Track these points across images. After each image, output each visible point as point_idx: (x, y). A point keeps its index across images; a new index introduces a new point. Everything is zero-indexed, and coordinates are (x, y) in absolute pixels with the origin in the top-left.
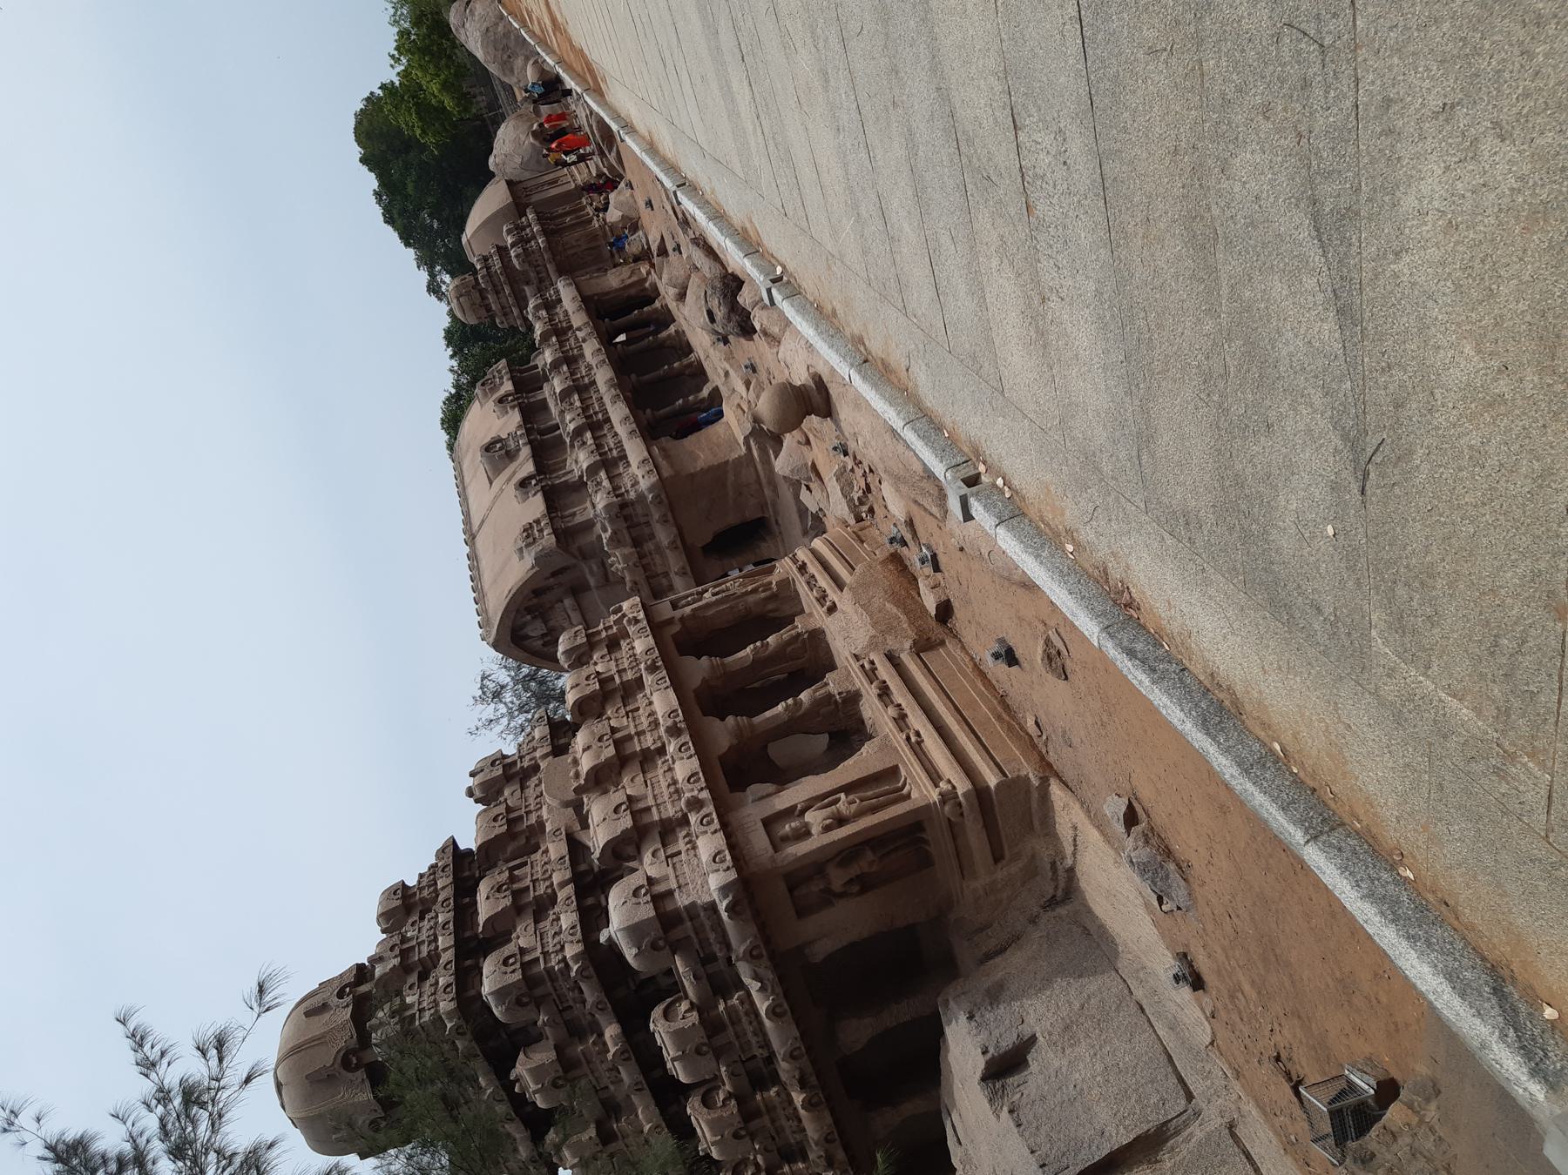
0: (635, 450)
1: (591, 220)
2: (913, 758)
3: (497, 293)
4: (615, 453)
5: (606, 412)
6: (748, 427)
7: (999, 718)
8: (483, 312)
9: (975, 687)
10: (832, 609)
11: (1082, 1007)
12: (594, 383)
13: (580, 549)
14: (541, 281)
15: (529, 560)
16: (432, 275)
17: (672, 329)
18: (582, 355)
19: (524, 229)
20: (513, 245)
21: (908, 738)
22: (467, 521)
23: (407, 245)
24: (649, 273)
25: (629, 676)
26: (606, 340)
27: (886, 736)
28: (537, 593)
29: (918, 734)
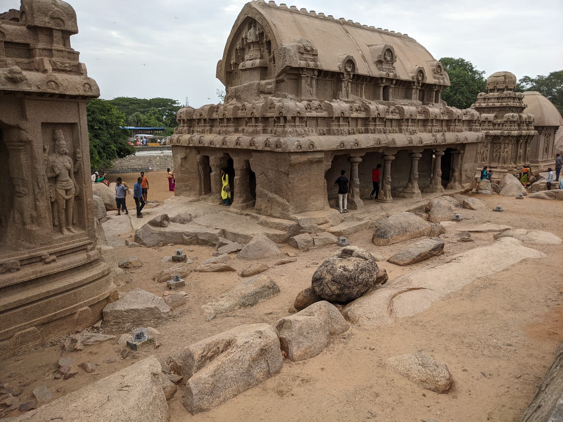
0: (328, 142)
1: (515, 163)
3: (498, 98)
4: (335, 128)
5: (374, 132)
6: (306, 225)
8: (491, 87)
12: (401, 131)
13: (283, 81)
14: (494, 125)
15: (286, 44)
16: (532, 81)
17: (417, 191)
18: (425, 131)
19: (527, 125)
20: (520, 117)
22: (357, 26)
23: (552, 74)
24: (463, 187)
26: (428, 150)
28: (269, 43)
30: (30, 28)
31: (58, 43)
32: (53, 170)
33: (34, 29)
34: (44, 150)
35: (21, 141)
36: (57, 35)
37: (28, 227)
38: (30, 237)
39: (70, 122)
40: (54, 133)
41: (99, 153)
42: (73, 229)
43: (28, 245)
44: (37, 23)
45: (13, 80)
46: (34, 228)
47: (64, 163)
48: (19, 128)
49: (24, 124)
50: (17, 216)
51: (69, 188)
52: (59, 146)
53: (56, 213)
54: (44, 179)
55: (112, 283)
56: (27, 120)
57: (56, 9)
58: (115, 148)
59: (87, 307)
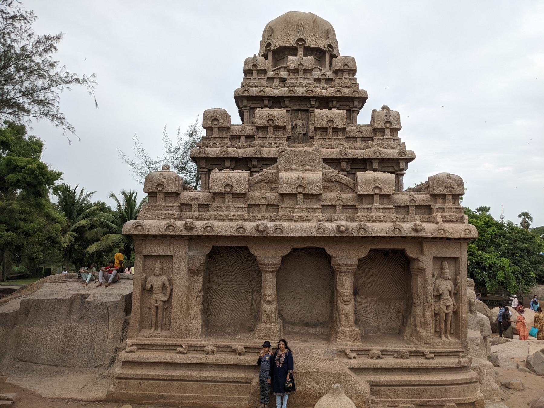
2: (165, 342)
7: (162, 397)
9: (196, 398)
10: (342, 353)
11: (73, 346)
21: (180, 346)
25: (360, 214)
27: (196, 337)
29: (180, 352)
30: (431, 195)
31: (449, 203)
32: (438, 291)
33: (434, 196)
34: (433, 275)
35: (419, 269)
36: (449, 198)
37: (418, 329)
38: (418, 336)
39: (454, 256)
40: (441, 264)
41: (517, 279)
42: (449, 337)
43: (416, 342)
44: (435, 192)
45: (416, 230)
46: (421, 330)
47: (446, 286)
48: (418, 260)
49: (421, 258)
50: (412, 320)
51: (448, 304)
52: (444, 273)
53: (438, 322)
54: (431, 296)
55: (479, 391)
56: (424, 255)
57: (449, 181)
58: (534, 275)
59: (454, 404)
